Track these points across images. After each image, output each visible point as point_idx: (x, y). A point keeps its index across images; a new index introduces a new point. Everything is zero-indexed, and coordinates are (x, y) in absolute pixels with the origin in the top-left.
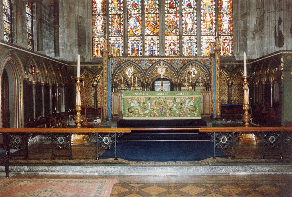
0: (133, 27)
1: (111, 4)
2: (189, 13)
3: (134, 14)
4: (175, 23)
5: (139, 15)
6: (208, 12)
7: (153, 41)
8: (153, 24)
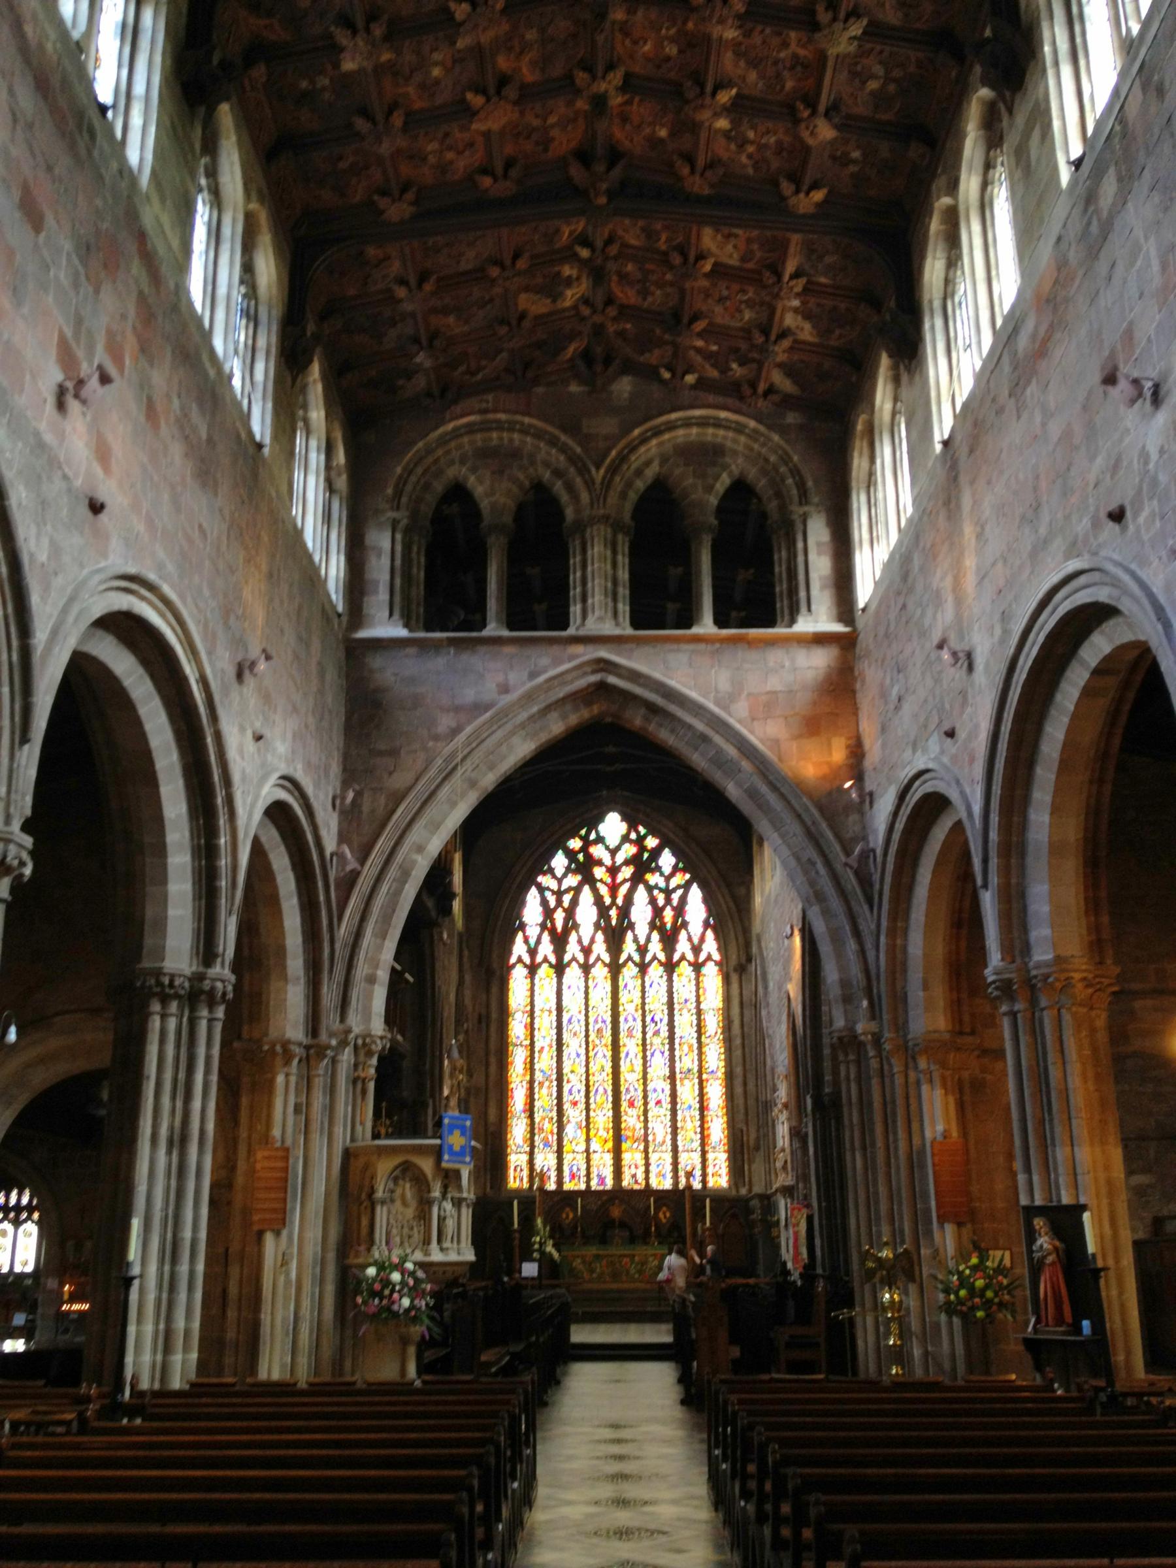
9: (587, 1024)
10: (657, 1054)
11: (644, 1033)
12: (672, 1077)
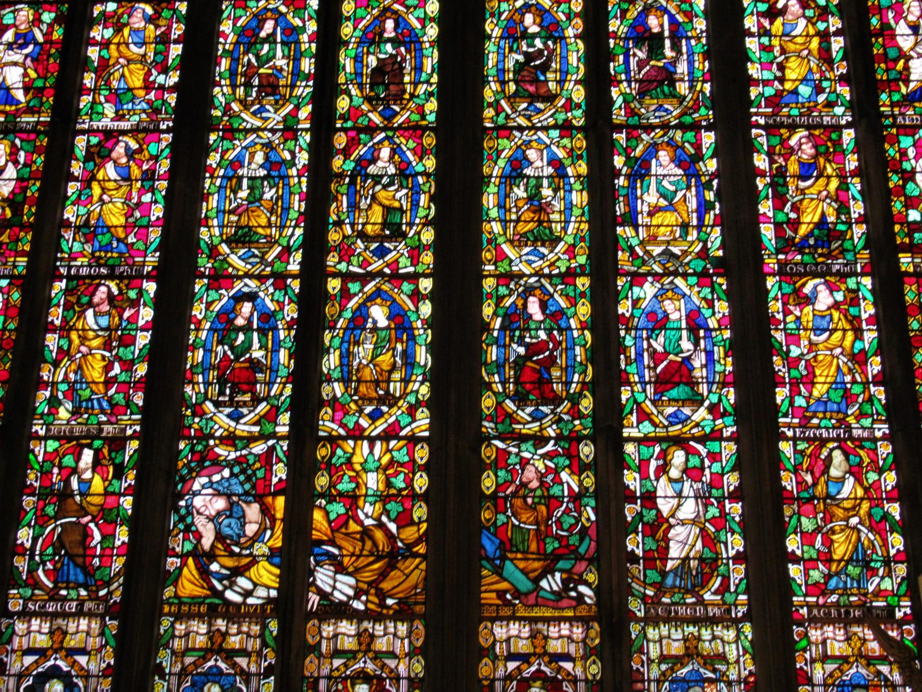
0: (207, 542)
1: (56, 364)
2: (680, 442)
3: (230, 439)
4: (567, 512)
5: (272, 449)
6: (833, 434)
7: (370, 667)
8: (381, 526)
9: (329, 41)
10: (664, 165)
11: (598, 81)
12: (739, 267)
